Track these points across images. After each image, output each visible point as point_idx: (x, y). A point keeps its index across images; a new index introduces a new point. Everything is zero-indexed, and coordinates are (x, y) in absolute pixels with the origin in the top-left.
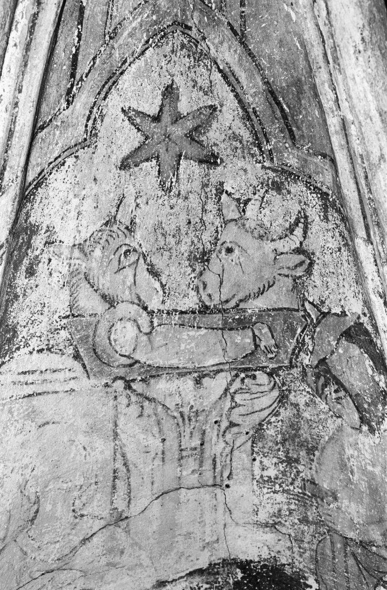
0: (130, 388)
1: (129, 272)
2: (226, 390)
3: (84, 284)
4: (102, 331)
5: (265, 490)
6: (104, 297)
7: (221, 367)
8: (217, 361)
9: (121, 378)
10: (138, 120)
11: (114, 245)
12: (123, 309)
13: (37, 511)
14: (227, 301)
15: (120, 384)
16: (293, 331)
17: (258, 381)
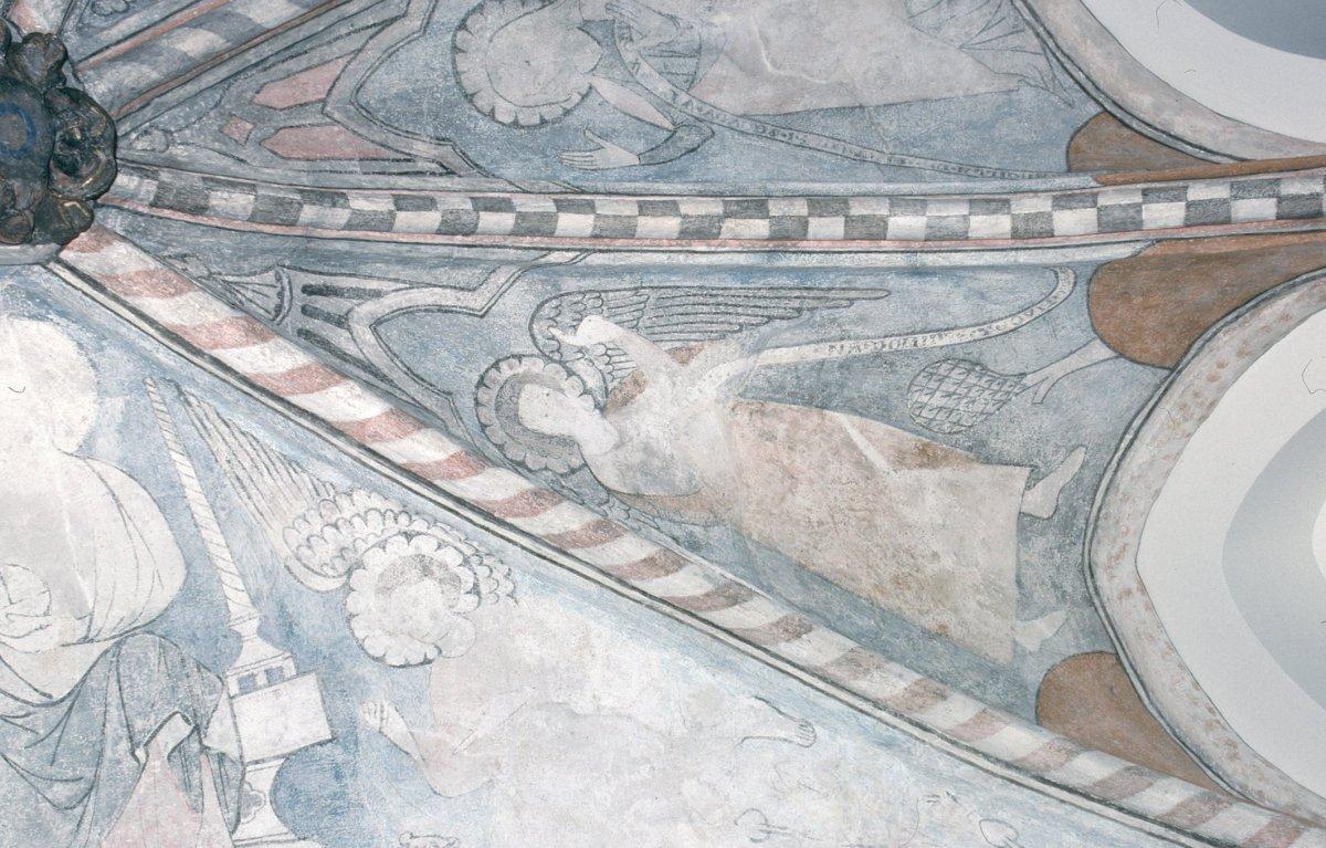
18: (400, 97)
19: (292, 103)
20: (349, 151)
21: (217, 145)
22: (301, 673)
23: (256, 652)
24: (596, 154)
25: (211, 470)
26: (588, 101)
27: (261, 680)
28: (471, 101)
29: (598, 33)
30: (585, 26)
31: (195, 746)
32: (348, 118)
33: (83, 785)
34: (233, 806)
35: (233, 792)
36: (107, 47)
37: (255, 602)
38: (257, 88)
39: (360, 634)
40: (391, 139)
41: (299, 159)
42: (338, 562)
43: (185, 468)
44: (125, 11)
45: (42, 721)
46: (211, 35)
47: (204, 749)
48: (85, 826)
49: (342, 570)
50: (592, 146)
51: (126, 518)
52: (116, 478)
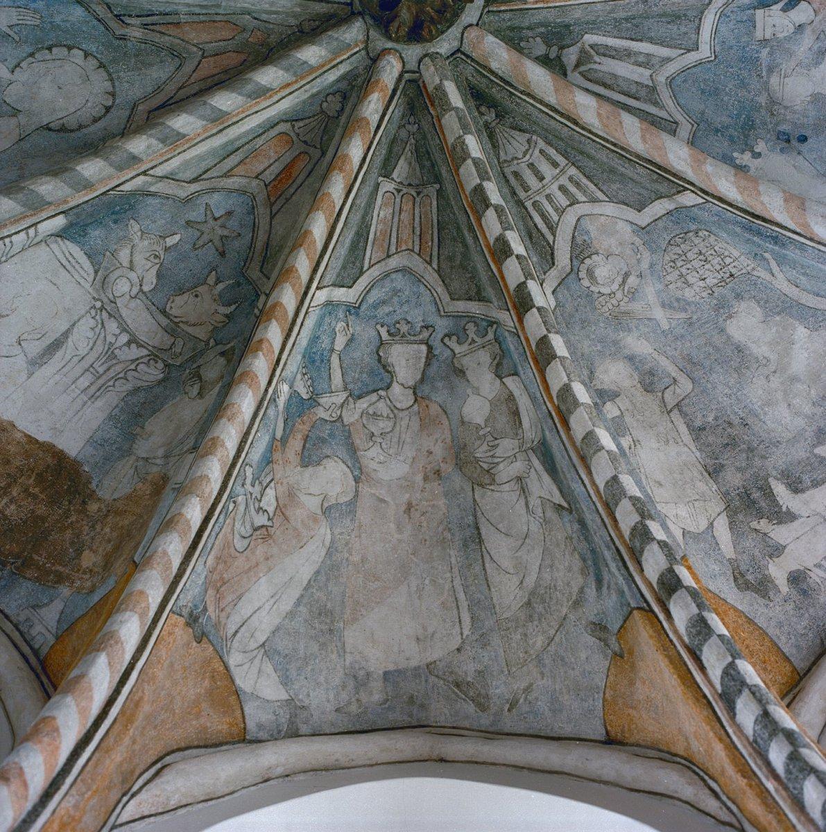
0: (101, 311)
1: (150, 264)
2: (137, 359)
3: (129, 247)
4: (117, 273)
5: (111, 423)
6: (131, 261)
7: (146, 345)
8: (147, 341)
9: (102, 302)
10: (208, 212)
11: (155, 247)
12: (133, 275)
13: (7, 315)
14: (176, 317)
15: (98, 304)
16: (194, 350)
17: (157, 365)
18: (151, 65)
19: (223, 56)
20: (187, 28)
21: (271, 26)
24: (15, 21)
26: (15, 62)
28: (101, 63)
29: (5, 108)
30: (15, 112)
32: (184, 48)
36: (348, 58)
38: (245, 63)
40: (157, 38)
41: (220, 21)
44: (328, 95)
46: (299, 55)
50: (16, 29)
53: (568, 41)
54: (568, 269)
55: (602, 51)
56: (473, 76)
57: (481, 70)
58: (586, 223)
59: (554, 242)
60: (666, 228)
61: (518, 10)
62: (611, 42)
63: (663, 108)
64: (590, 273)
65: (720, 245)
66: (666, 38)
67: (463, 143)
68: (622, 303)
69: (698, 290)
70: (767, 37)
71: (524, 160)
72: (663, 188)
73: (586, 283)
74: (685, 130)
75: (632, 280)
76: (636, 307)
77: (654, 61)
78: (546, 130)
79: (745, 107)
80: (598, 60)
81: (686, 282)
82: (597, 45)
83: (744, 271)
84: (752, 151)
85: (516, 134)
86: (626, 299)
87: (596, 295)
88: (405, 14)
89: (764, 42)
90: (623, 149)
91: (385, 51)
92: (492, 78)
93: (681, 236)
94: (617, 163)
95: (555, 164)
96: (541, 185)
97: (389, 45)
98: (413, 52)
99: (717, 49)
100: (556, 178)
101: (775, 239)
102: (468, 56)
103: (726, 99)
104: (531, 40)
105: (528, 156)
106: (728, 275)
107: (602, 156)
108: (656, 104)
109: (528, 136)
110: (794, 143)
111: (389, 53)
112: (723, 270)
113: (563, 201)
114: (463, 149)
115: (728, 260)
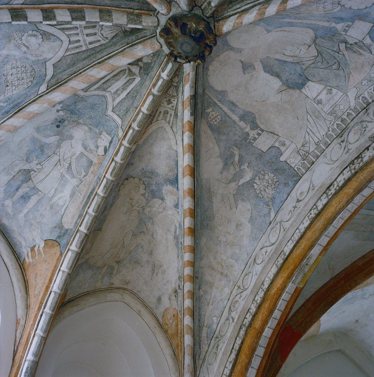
22: (353, 22)
23: (340, 27)
25: (291, 16)
27: (347, 28)
31: (349, 46)
33: (337, 63)
34: (367, 49)
35: (364, 48)
37: (328, 21)
39: (356, 8)
42: (334, 5)
43: (287, 20)
45: (319, 59)
47: (351, 44)
48: (344, 69)
49: (337, 5)
51: (290, 31)
52: (279, 29)
53: (142, 71)
54: (39, 28)
55: (130, 81)
56: (145, 33)
57: (144, 38)
58: (59, 43)
59: (56, 28)
60: (41, 71)
61: (162, 64)
62: (132, 86)
63: (95, 90)
64: (35, 36)
65: (21, 88)
66: (122, 104)
67: (109, 22)
68: (16, 41)
69: (9, 71)
70: (102, 135)
71: (99, 33)
72: (53, 81)
73: (30, 32)
74: (82, 94)
75: (24, 49)
76: (11, 46)
77: (116, 96)
78: (105, 48)
79: (81, 114)
80: (127, 78)
81: (14, 68)
82: (134, 81)
83: (6, 91)
84: (60, 110)
85: (113, 34)
86: (16, 43)
87: (23, 34)
88: (176, 31)
89: (101, 133)
90: (77, 75)
91: (169, 10)
92: (138, 41)
93: (34, 75)
94: (74, 69)
95: (91, 43)
96: (84, 34)
97: (171, 14)
98: (163, 20)
99: (108, 117)
100: (85, 41)
101: (7, 112)
102: (152, 37)
103: (88, 110)
104: (152, 58)
105: (100, 35)
106: (8, 85)
107: (80, 65)
108: (98, 88)
109: (110, 39)
110: (59, 123)
111: (167, 12)
112: (11, 84)
113: (73, 39)
114: (106, 20)
115: (14, 88)
